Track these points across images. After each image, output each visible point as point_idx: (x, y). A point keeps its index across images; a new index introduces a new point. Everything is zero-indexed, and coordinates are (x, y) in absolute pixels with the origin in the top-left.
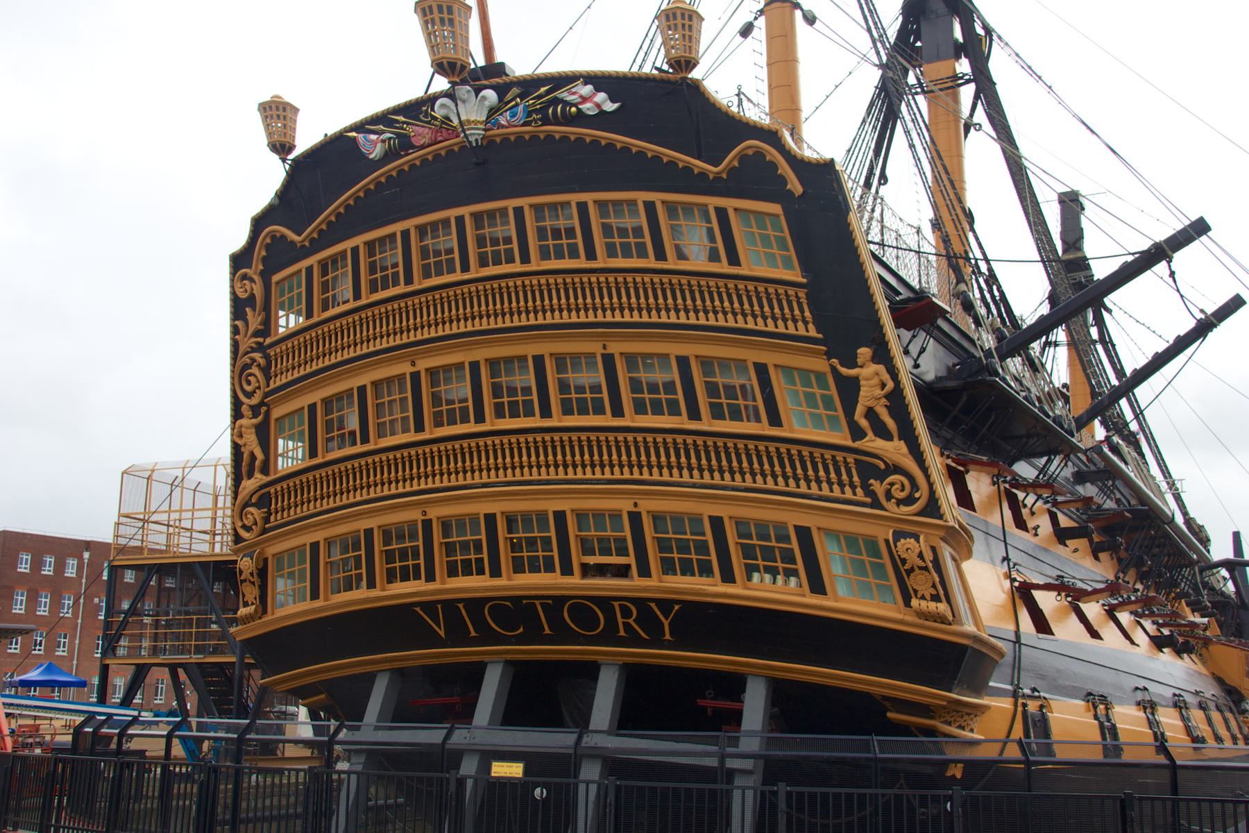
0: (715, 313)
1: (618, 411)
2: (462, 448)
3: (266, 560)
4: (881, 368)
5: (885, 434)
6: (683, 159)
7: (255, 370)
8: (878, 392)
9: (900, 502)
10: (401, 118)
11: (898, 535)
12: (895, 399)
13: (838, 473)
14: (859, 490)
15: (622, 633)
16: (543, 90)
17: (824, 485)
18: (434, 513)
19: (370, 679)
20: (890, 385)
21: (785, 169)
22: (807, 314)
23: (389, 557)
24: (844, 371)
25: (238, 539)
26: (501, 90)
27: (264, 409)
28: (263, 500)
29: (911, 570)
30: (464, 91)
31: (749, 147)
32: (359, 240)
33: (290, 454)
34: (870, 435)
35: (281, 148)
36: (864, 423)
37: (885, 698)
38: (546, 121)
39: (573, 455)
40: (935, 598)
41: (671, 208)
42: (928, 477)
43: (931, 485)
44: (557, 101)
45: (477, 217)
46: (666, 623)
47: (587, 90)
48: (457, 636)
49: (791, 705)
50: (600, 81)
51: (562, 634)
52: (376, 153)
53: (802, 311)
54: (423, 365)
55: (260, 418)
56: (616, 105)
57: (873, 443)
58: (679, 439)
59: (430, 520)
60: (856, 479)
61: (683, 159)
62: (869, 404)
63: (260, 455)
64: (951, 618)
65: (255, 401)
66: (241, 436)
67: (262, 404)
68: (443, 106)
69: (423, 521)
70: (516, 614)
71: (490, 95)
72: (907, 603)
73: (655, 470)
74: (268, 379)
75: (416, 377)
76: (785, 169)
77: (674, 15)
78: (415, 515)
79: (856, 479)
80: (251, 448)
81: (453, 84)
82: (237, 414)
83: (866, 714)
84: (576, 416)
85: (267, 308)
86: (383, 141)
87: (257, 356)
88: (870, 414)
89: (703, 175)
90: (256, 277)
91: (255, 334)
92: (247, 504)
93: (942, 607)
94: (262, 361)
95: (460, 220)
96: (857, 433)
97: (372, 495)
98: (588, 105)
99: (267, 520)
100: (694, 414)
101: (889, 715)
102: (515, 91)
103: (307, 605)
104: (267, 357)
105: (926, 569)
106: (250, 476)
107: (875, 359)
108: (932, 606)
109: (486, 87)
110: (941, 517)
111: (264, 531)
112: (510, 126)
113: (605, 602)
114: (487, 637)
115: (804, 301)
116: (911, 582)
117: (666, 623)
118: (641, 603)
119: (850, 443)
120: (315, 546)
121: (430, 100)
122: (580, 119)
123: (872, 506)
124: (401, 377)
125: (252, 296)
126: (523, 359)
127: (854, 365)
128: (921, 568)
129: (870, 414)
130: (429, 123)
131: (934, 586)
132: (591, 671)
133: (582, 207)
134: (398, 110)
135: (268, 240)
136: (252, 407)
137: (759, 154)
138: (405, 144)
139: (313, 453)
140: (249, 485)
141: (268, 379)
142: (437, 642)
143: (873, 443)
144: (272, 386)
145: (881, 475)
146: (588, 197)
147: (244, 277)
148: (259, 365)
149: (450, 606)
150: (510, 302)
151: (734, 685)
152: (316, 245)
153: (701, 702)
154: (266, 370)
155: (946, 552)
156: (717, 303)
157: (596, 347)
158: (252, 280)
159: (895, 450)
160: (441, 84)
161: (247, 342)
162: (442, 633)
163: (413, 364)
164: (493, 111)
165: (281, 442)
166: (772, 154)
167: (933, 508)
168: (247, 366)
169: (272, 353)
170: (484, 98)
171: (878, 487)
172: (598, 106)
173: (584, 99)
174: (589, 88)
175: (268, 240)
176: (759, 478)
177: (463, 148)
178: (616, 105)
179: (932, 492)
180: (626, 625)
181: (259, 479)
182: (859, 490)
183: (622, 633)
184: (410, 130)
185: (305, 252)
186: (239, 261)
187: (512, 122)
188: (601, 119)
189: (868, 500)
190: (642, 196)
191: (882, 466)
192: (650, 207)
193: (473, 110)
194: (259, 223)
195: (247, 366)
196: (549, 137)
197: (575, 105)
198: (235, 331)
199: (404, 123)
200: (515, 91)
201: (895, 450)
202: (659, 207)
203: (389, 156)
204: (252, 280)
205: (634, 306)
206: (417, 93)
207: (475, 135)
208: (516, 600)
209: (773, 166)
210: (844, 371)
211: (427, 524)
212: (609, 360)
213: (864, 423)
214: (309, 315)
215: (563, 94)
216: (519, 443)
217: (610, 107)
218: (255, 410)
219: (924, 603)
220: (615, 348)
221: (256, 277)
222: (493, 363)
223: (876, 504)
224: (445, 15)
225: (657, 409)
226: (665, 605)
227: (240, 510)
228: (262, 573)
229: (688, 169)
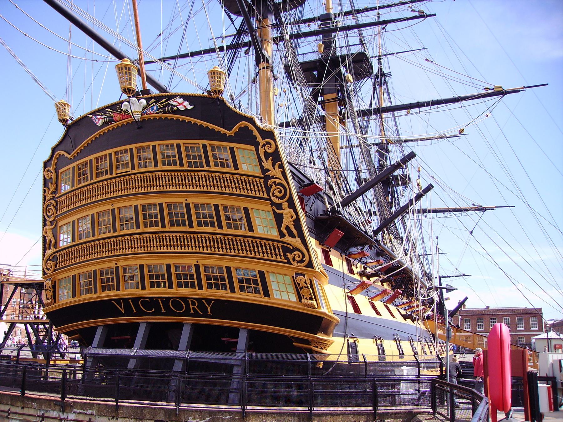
0: (229, 188)
1: (191, 226)
2: (131, 239)
3: (55, 282)
4: (291, 210)
5: (292, 235)
6: (217, 128)
7: (52, 207)
8: (290, 220)
9: (298, 262)
11: (297, 274)
12: (297, 222)
13: (275, 251)
14: (283, 257)
15: (192, 312)
16: (163, 100)
17: (270, 255)
18: (120, 264)
19: (95, 328)
20: (295, 217)
21: (256, 133)
22: (264, 189)
23: (103, 281)
24: (277, 211)
25: (44, 273)
26: (148, 100)
28: (53, 257)
29: (302, 288)
30: (134, 99)
31: (242, 124)
32: (92, 157)
33: (65, 239)
34: (287, 235)
35: (64, 121)
36: (285, 231)
37: (292, 337)
38: (165, 112)
39: (174, 242)
40: (311, 299)
41: (213, 148)
42: (308, 252)
43: (310, 255)
44: (169, 105)
45: (138, 149)
46: (209, 308)
47: (180, 101)
48: (129, 312)
49: (257, 341)
50: (186, 97)
51: (169, 312)
52: (100, 123)
53: (262, 187)
54: (116, 206)
56: (192, 107)
57: (287, 239)
58: (214, 236)
60: (281, 253)
61: (217, 128)
62: (287, 224)
63: (53, 241)
64: (316, 307)
65: (51, 220)
66: (46, 233)
67: (54, 220)
68: (125, 105)
70: (151, 304)
71: (144, 102)
72: (300, 301)
73: (205, 248)
74: (57, 210)
75: (113, 210)
76: (256, 133)
77: (214, 73)
78: (113, 265)
79: (281, 253)
81: (129, 97)
82: (45, 225)
83: (286, 344)
84: (176, 227)
85: (57, 182)
86: (102, 119)
87: (52, 201)
88: (287, 228)
89: (225, 134)
91: (52, 193)
92: (48, 259)
93: (314, 302)
94: (55, 204)
95: (131, 150)
96: (282, 235)
98: (181, 106)
99: (56, 266)
100: (220, 227)
101: (294, 344)
102: (153, 100)
103: (71, 299)
104: (56, 202)
105: (307, 287)
107: (289, 207)
108: (310, 302)
109: (142, 98)
110: (313, 268)
111: (55, 270)
112: (151, 114)
113: (185, 300)
114: (140, 313)
115: (263, 184)
116: (302, 293)
117: (209, 308)
118: (199, 300)
119: (279, 239)
120: (74, 277)
121: (121, 103)
122: (178, 112)
123: (287, 263)
126: (155, 205)
127: (281, 209)
128: (305, 287)
129: (287, 228)
131: (310, 294)
132: (179, 326)
133: (178, 146)
134: (108, 107)
135: (58, 156)
136: (50, 222)
137: (246, 127)
138: (110, 121)
139: (73, 240)
140: (49, 252)
141: (57, 210)
142: (121, 315)
143: (287, 239)
144: (58, 213)
145: (291, 251)
146: (181, 142)
147: (48, 171)
149: (126, 300)
150: (150, 182)
151: (235, 332)
152: (75, 159)
153: (223, 339)
154: (55, 207)
155: (315, 282)
156: (229, 184)
157: (183, 200)
158: (51, 172)
159: (296, 242)
160: (125, 97)
161: (48, 197)
163: (113, 205)
164: (144, 108)
165: (62, 236)
166: (251, 127)
167: (310, 265)
168: (48, 206)
170: (141, 103)
171: (290, 256)
172: (185, 107)
173: (180, 104)
174: (182, 100)
175: (58, 156)
176: (245, 252)
177: (133, 122)
178: (192, 107)
179: (310, 258)
180: (194, 309)
181: (52, 250)
182: (283, 257)
183: (192, 312)
184: (112, 115)
186: (46, 164)
187: (152, 113)
188: (186, 112)
189: (286, 261)
190: (201, 142)
191: (292, 248)
192: (204, 146)
193: (136, 107)
194: (54, 150)
195: (48, 206)
196: (166, 118)
197: (176, 106)
198: (45, 191)
200: (153, 100)
201: (296, 242)
202: (208, 146)
203: (105, 124)
205: (198, 184)
206: (116, 100)
207: (138, 117)
208: (151, 298)
209: (252, 131)
210: (277, 211)
211: (117, 268)
212: (188, 205)
213: (285, 231)
214: (73, 186)
215: (171, 102)
216: (153, 237)
217: (190, 107)
219: (306, 301)
220: (191, 201)
222: (143, 206)
223: (289, 263)
224: (128, 71)
225: (206, 225)
226: (209, 301)
227: (46, 261)
228: (54, 287)
229: (219, 132)
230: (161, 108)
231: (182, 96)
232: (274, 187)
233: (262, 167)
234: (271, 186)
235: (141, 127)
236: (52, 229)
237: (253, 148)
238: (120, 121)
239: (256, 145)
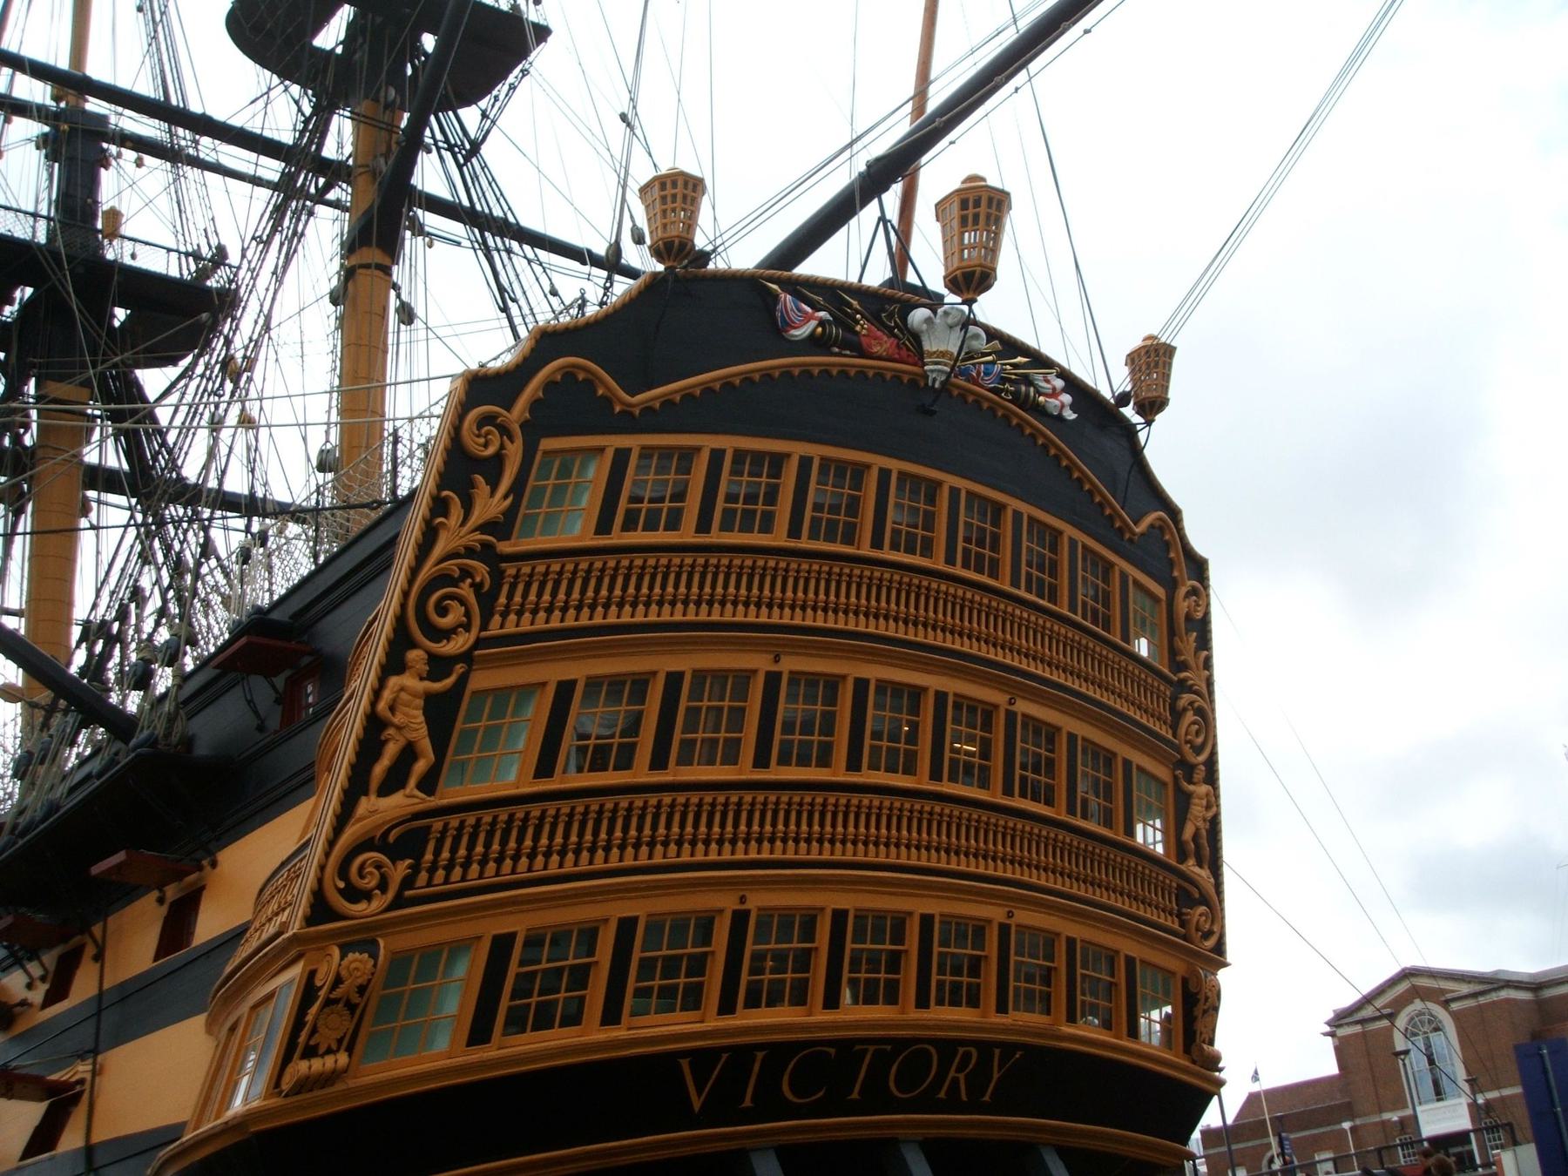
7: (465, 590)
10: (855, 303)
16: (1020, 359)
27: (460, 668)
28: (405, 841)
44: (1028, 381)
47: (1059, 383)
48: (723, 1109)
50: (1073, 385)
52: (801, 333)
54: (789, 664)
55: (449, 682)
56: (1074, 416)
57: (1191, 867)
59: (748, 912)
67: (467, 657)
69: (735, 912)
80: (412, 736)
87: (481, 570)
90: (516, 429)
96: (1182, 856)
97: (658, 860)
104: (497, 576)
106: (386, 790)
113: (947, 1047)
117: (996, 1076)
122: (1040, 411)
123: (1185, 938)
124: (746, 676)
125: (499, 459)
127: (1190, 782)
130: (890, 330)
136: (433, 658)
148: (477, 587)
154: (487, 601)
162: (697, 1104)
169: (512, 571)
177: (913, 383)
178: (1074, 416)
185: (629, 423)
199: (858, 312)
203: (815, 343)
204: (505, 431)
207: (936, 372)
215: (1037, 375)
217: (1070, 415)
218: (438, 666)
221: (516, 429)
230: (1010, 381)
231: (1064, 374)
232: (1190, 716)
233: (1173, 652)
234: (1185, 710)
235: (927, 412)
236: (431, 701)
237: (1160, 591)
238: (880, 358)
239: (1171, 585)
